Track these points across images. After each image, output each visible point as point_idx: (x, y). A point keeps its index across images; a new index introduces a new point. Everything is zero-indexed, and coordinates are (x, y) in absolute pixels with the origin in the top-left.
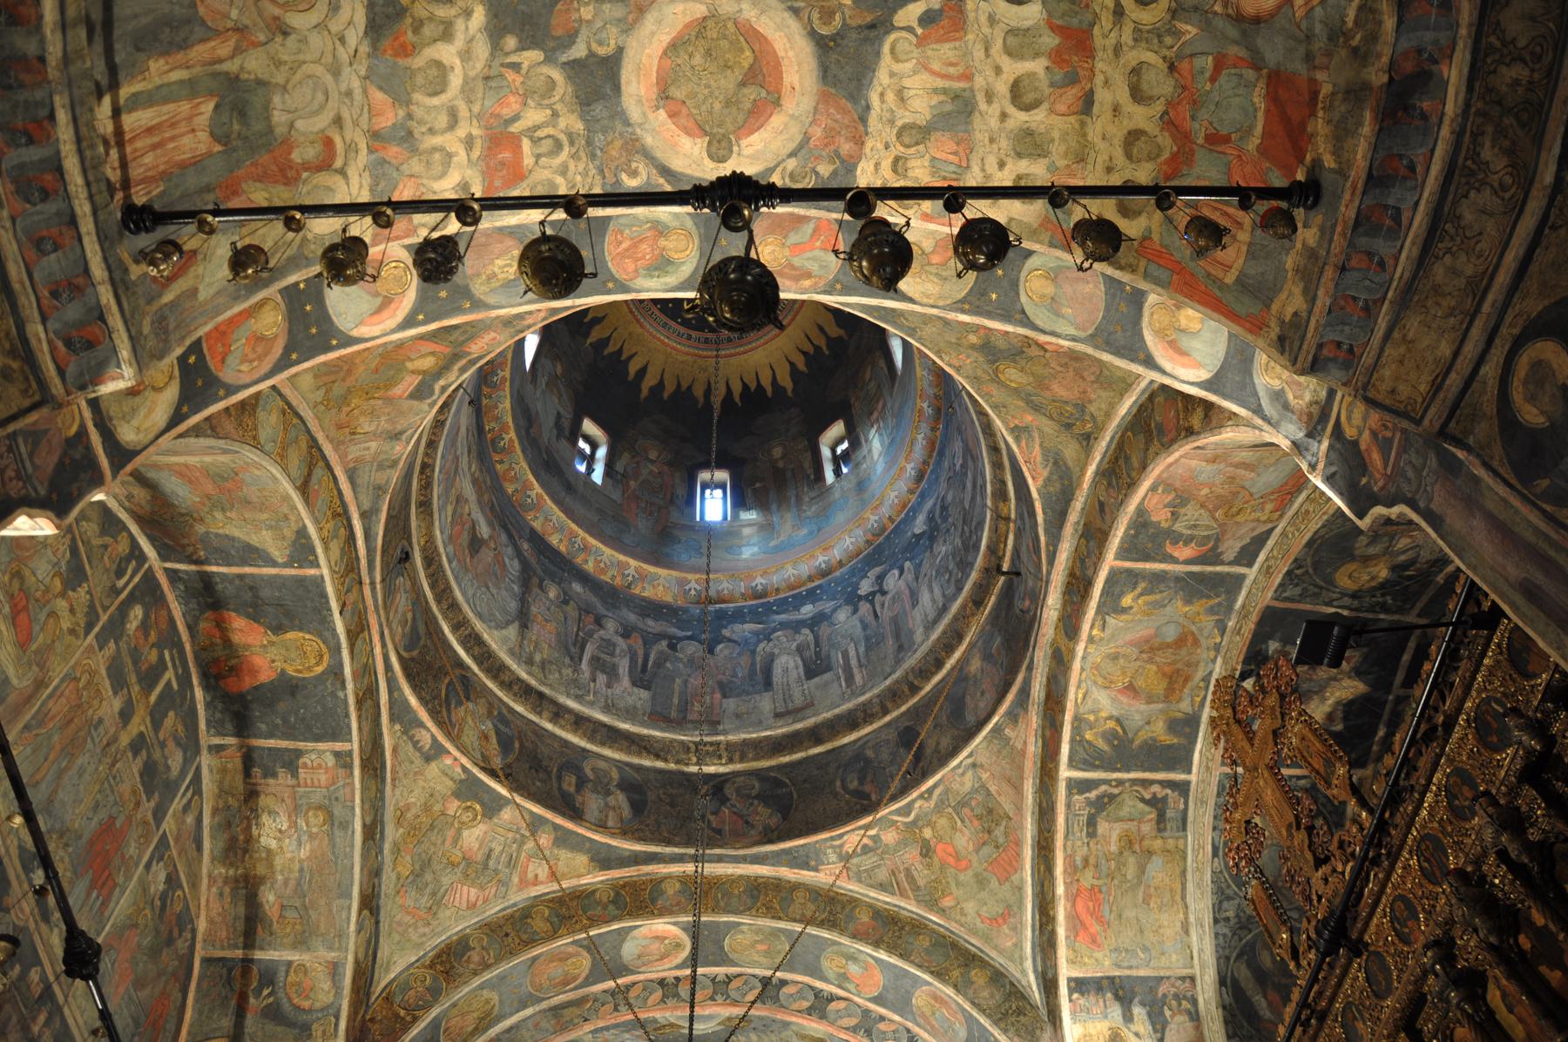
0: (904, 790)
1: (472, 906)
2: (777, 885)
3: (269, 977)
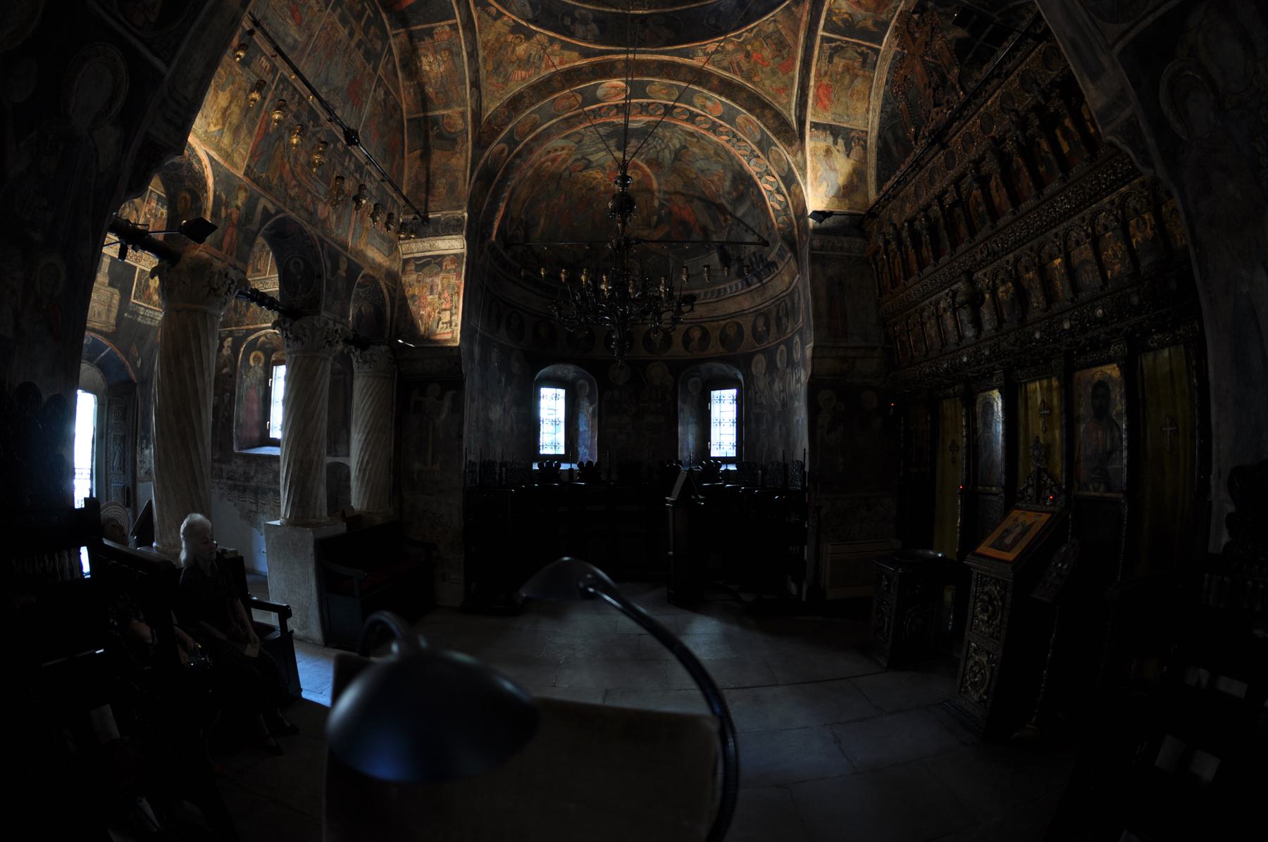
0: (738, 28)
1: (523, 79)
2: (673, 64)
3: (435, 121)
